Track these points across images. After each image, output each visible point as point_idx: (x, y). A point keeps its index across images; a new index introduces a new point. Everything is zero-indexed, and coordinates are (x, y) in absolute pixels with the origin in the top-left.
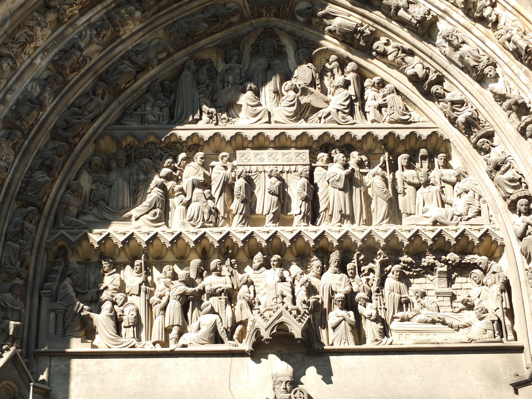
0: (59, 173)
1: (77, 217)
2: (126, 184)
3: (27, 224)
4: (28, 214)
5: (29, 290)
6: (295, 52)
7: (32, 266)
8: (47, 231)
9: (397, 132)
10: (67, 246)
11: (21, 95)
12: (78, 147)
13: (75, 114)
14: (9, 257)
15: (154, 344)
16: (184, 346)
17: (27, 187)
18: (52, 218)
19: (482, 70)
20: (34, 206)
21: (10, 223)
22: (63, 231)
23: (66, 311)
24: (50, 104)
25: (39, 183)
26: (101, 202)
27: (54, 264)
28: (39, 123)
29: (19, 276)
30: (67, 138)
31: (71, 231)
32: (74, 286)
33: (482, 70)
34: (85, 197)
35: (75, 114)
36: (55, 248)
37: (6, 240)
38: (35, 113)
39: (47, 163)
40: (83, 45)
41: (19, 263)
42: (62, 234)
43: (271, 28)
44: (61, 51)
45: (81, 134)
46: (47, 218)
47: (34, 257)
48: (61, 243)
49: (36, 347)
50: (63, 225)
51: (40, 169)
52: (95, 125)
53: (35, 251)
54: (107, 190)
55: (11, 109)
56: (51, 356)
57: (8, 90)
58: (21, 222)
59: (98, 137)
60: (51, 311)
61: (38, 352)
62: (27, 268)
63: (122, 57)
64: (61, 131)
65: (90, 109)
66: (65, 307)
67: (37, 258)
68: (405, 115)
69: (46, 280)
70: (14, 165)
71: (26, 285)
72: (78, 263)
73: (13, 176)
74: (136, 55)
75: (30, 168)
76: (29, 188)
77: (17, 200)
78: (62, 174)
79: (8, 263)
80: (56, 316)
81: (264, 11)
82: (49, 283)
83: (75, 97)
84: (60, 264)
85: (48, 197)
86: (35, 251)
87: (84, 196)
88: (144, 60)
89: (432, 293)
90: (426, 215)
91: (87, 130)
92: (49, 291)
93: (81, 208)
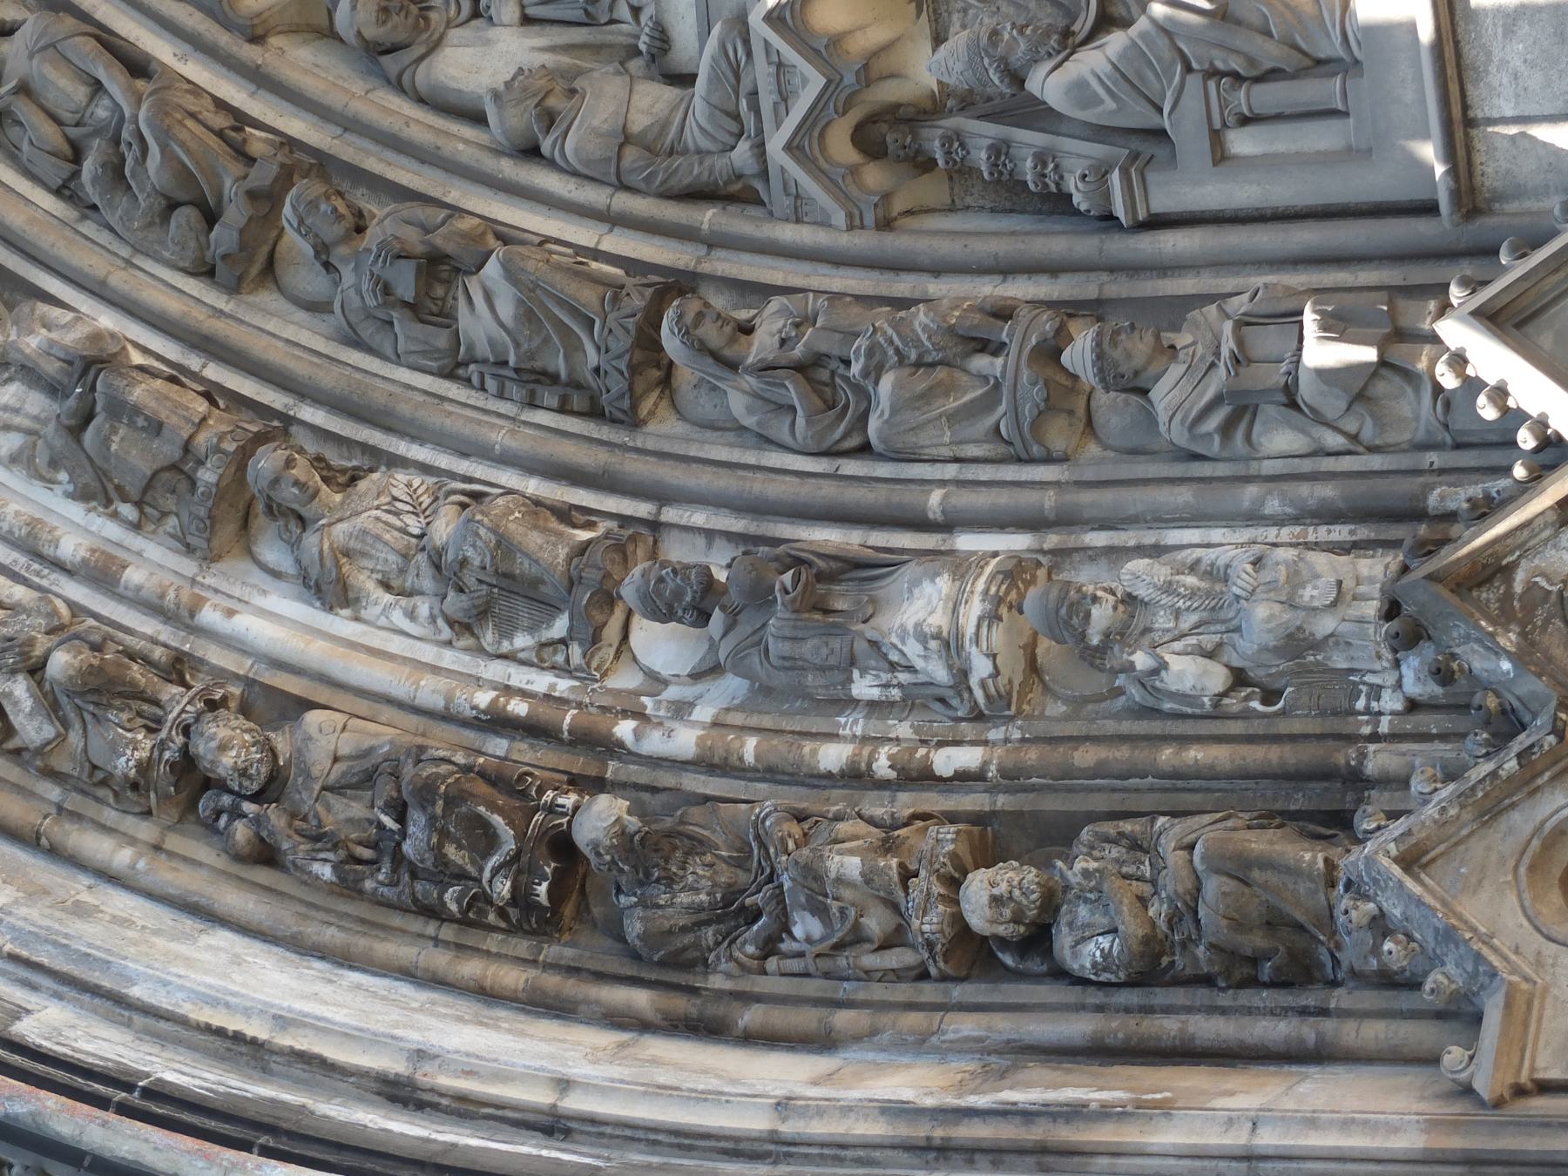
0: (456, 211)
1: (685, 80)
3: (762, 344)
4: (703, 349)
5: (1119, 288)
7: (989, 289)
8: (788, 233)
10: (855, 116)
11: (51, 482)
12: (297, 126)
13: (116, 173)
14: (953, 418)
17: (554, 379)
18: (707, 217)
20: (652, 321)
21: (768, 442)
22: (776, 144)
23: (1213, 73)
24: (79, 317)
25: (528, 315)
27: (961, 172)
28: (194, 362)
29: (1050, 352)
30: (253, 195)
31: (767, 101)
32: (1068, 43)
34: (568, 48)
35: (116, 173)
36: (875, 176)
37: (865, 450)
38: (140, 393)
39: (405, 283)
41: (981, 363)
42: (789, 148)
45: (221, 121)
46: (714, 242)
47: (936, 287)
48: (841, 147)
49: (1428, 209)
50: (742, 154)
51: (445, 318)
52: (160, 48)
53: (903, 286)
55: (136, 527)
56: (1470, 123)
57: (38, 556)
58: (751, 381)
59: (226, 24)
60: (1220, 155)
61: (1456, 196)
62: (1003, 313)
64: (223, 237)
65: (80, 93)
66: (1193, 81)
67: (938, 269)
69: (1057, 204)
70: (444, 461)
71: (1094, 309)
72: (938, 40)
73: (506, 460)
75: (449, 375)
76: (560, 365)
77: (633, 421)
78: (458, 193)
79: (989, 421)
80: (1245, 121)
82: (1072, 184)
84: (955, 139)
85: (597, 254)
86: (903, 286)
87: (565, 60)
91: (196, 90)
92: (1115, 177)
93: (636, 65)
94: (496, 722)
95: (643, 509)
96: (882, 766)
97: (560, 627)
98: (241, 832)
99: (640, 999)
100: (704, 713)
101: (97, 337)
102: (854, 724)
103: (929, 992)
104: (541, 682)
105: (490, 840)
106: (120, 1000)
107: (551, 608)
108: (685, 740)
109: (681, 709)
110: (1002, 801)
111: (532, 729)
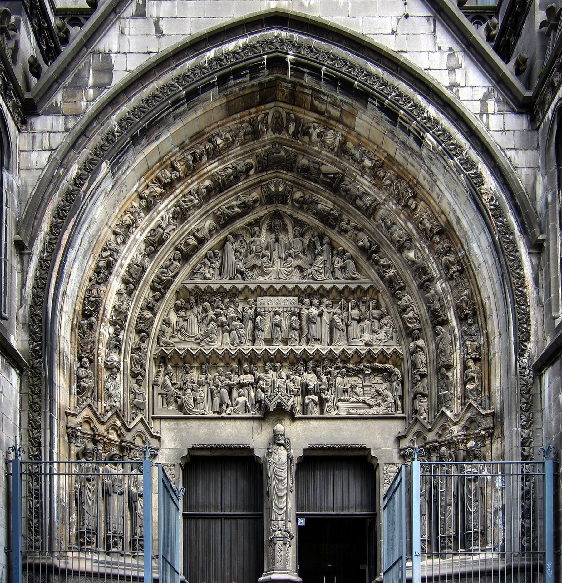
2: (196, 319)
3: (142, 344)
6: (293, 229)
9: (350, 285)
13: (163, 273)
15: (214, 413)
16: (229, 414)
18: (156, 340)
19: (403, 244)
22: (162, 348)
26: (182, 330)
31: (167, 348)
33: (403, 244)
39: (150, 305)
40: (164, 226)
43: (279, 211)
44: (152, 230)
50: (162, 344)
54: (186, 323)
62: (145, 370)
63: (189, 233)
64: (156, 285)
68: (355, 274)
74: (198, 232)
75: (141, 309)
81: (274, 199)
83: (163, 262)
88: (202, 236)
89: (361, 386)
90: (362, 339)
94: (104, 310)
95: (126, 329)
96: (99, 351)
97: (114, 318)
98: (93, 278)
99: (75, 322)
100: (105, 333)
101: (146, 269)
102: (104, 349)
103: (76, 354)
104: (109, 315)
105: (92, 307)
106: (74, 261)
107: (116, 317)
108: (102, 330)
109: (105, 330)
110: (96, 364)
111: (104, 313)
